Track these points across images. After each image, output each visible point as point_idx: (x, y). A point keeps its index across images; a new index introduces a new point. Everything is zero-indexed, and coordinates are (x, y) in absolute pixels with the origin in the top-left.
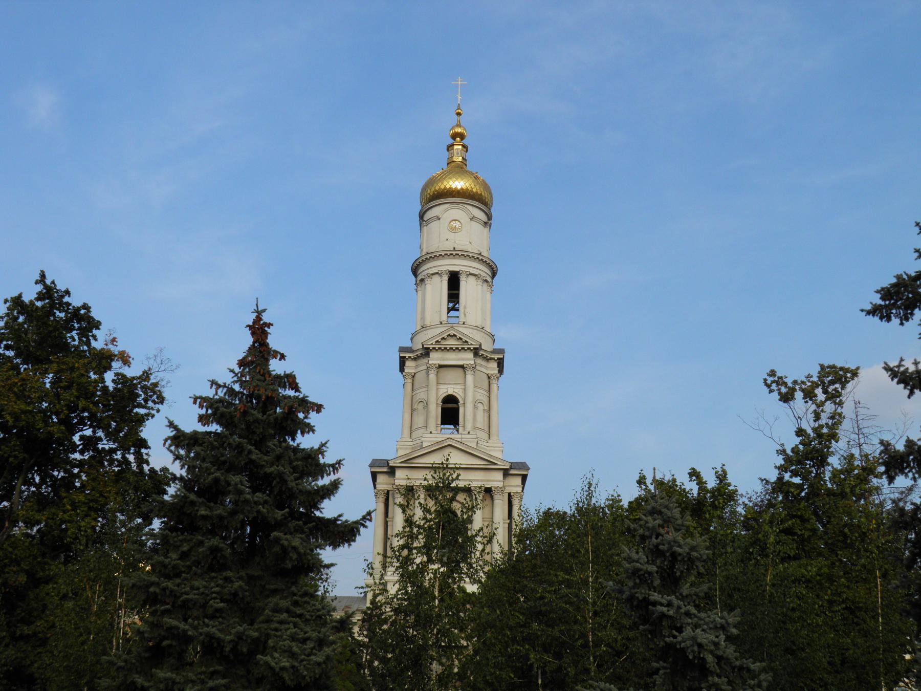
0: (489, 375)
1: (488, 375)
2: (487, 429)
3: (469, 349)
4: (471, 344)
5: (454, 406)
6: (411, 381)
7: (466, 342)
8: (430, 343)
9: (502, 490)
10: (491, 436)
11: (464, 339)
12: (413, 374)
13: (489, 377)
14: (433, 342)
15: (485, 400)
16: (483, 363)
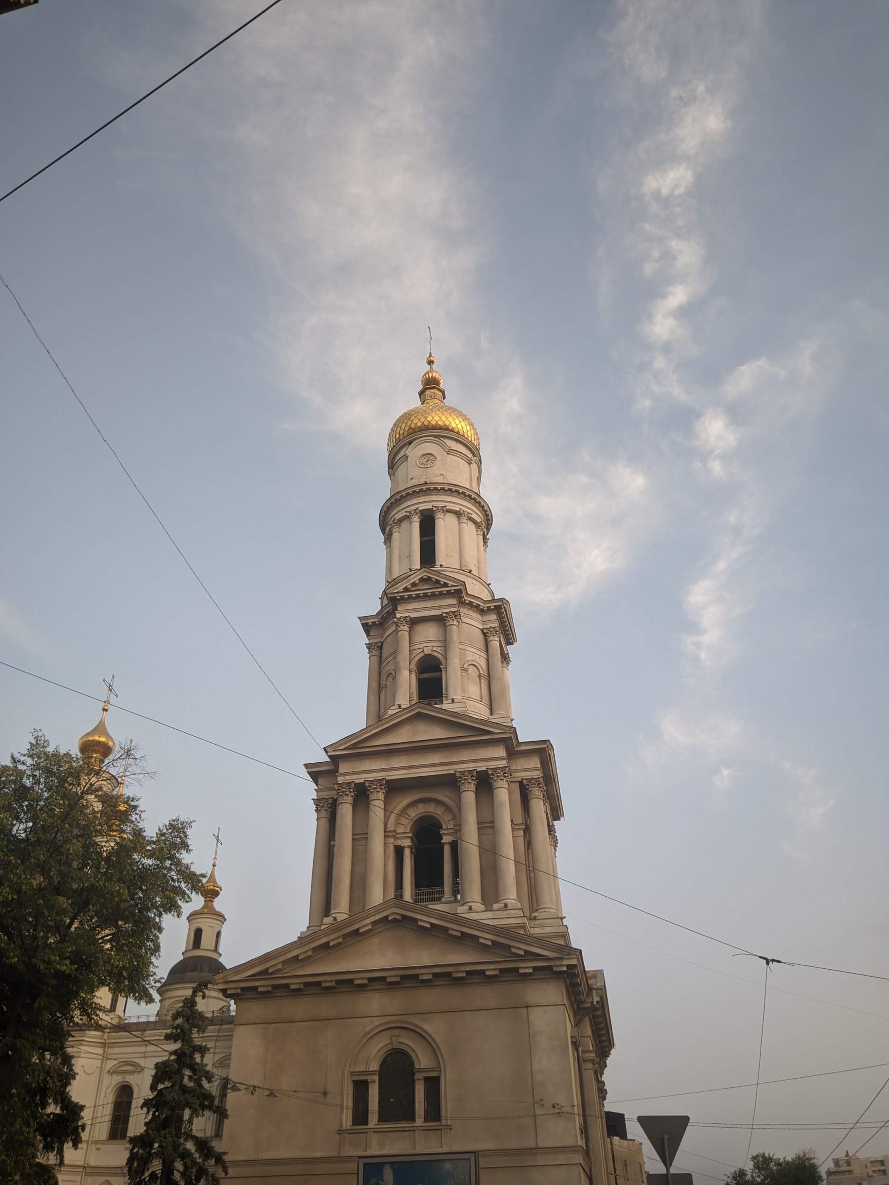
0: (485, 631)
1: (482, 630)
2: (486, 699)
3: (449, 592)
4: (453, 586)
5: (438, 674)
6: (377, 653)
7: (446, 585)
8: (397, 591)
9: (506, 772)
10: (494, 708)
11: (442, 581)
12: (379, 644)
13: (484, 634)
14: (401, 589)
15: (483, 664)
16: (476, 615)
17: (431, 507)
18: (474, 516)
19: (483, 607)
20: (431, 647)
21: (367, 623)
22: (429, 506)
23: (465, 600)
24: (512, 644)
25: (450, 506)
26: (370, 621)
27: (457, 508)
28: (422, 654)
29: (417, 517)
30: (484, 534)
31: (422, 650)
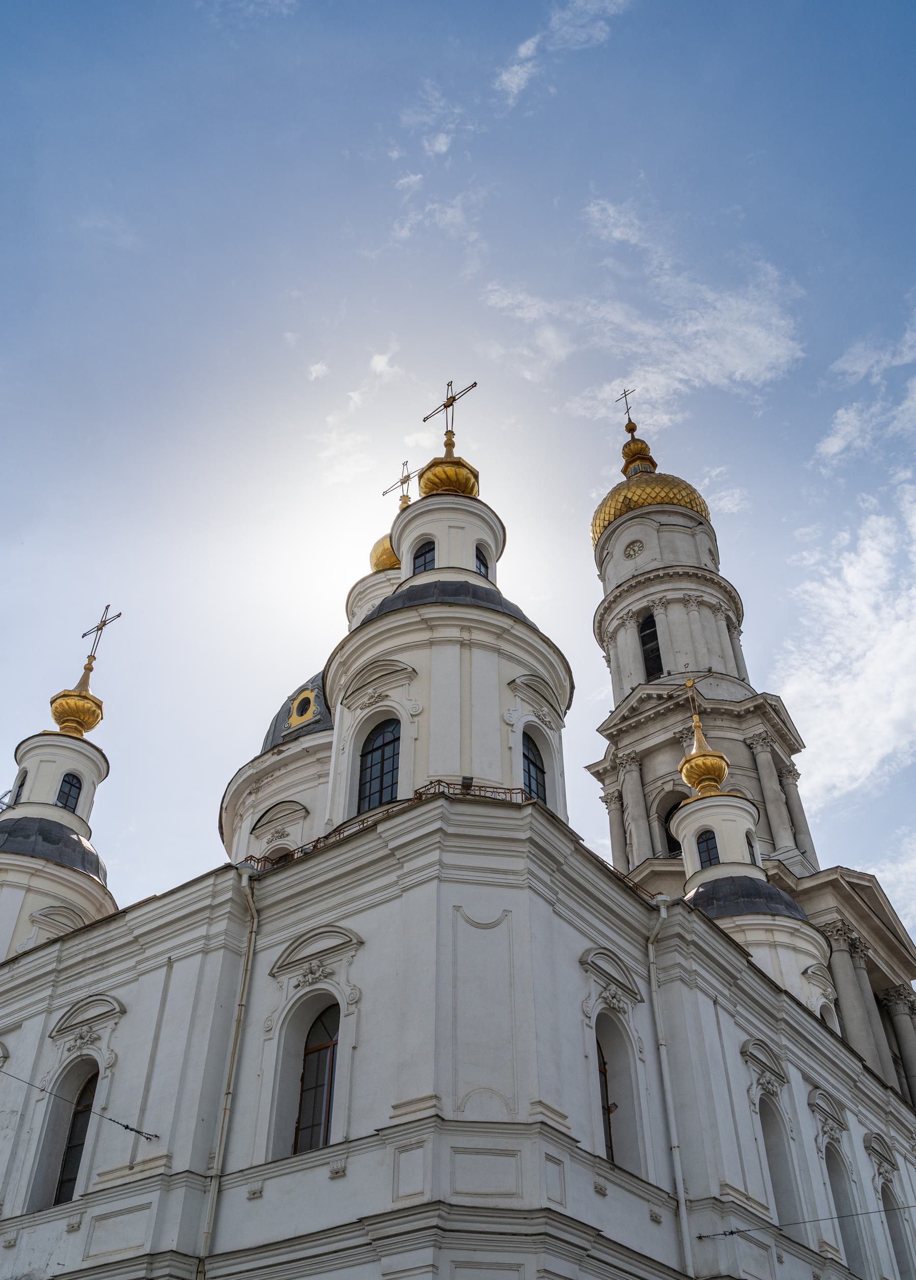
13: (750, 747)
17: (647, 604)
18: (707, 598)
19: (738, 712)
20: (672, 782)
21: (598, 771)
22: (644, 603)
23: (705, 709)
24: (798, 751)
25: (670, 595)
26: (600, 768)
27: (679, 595)
28: (663, 794)
29: (632, 622)
30: (728, 618)
31: (661, 788)
